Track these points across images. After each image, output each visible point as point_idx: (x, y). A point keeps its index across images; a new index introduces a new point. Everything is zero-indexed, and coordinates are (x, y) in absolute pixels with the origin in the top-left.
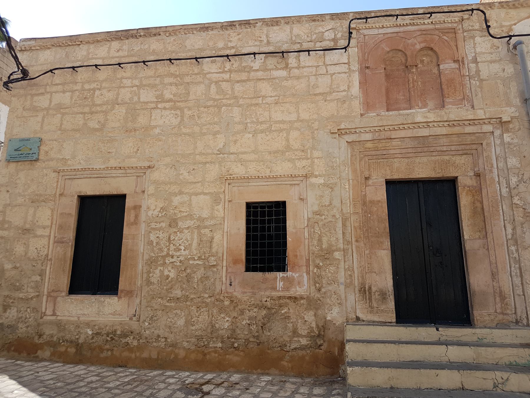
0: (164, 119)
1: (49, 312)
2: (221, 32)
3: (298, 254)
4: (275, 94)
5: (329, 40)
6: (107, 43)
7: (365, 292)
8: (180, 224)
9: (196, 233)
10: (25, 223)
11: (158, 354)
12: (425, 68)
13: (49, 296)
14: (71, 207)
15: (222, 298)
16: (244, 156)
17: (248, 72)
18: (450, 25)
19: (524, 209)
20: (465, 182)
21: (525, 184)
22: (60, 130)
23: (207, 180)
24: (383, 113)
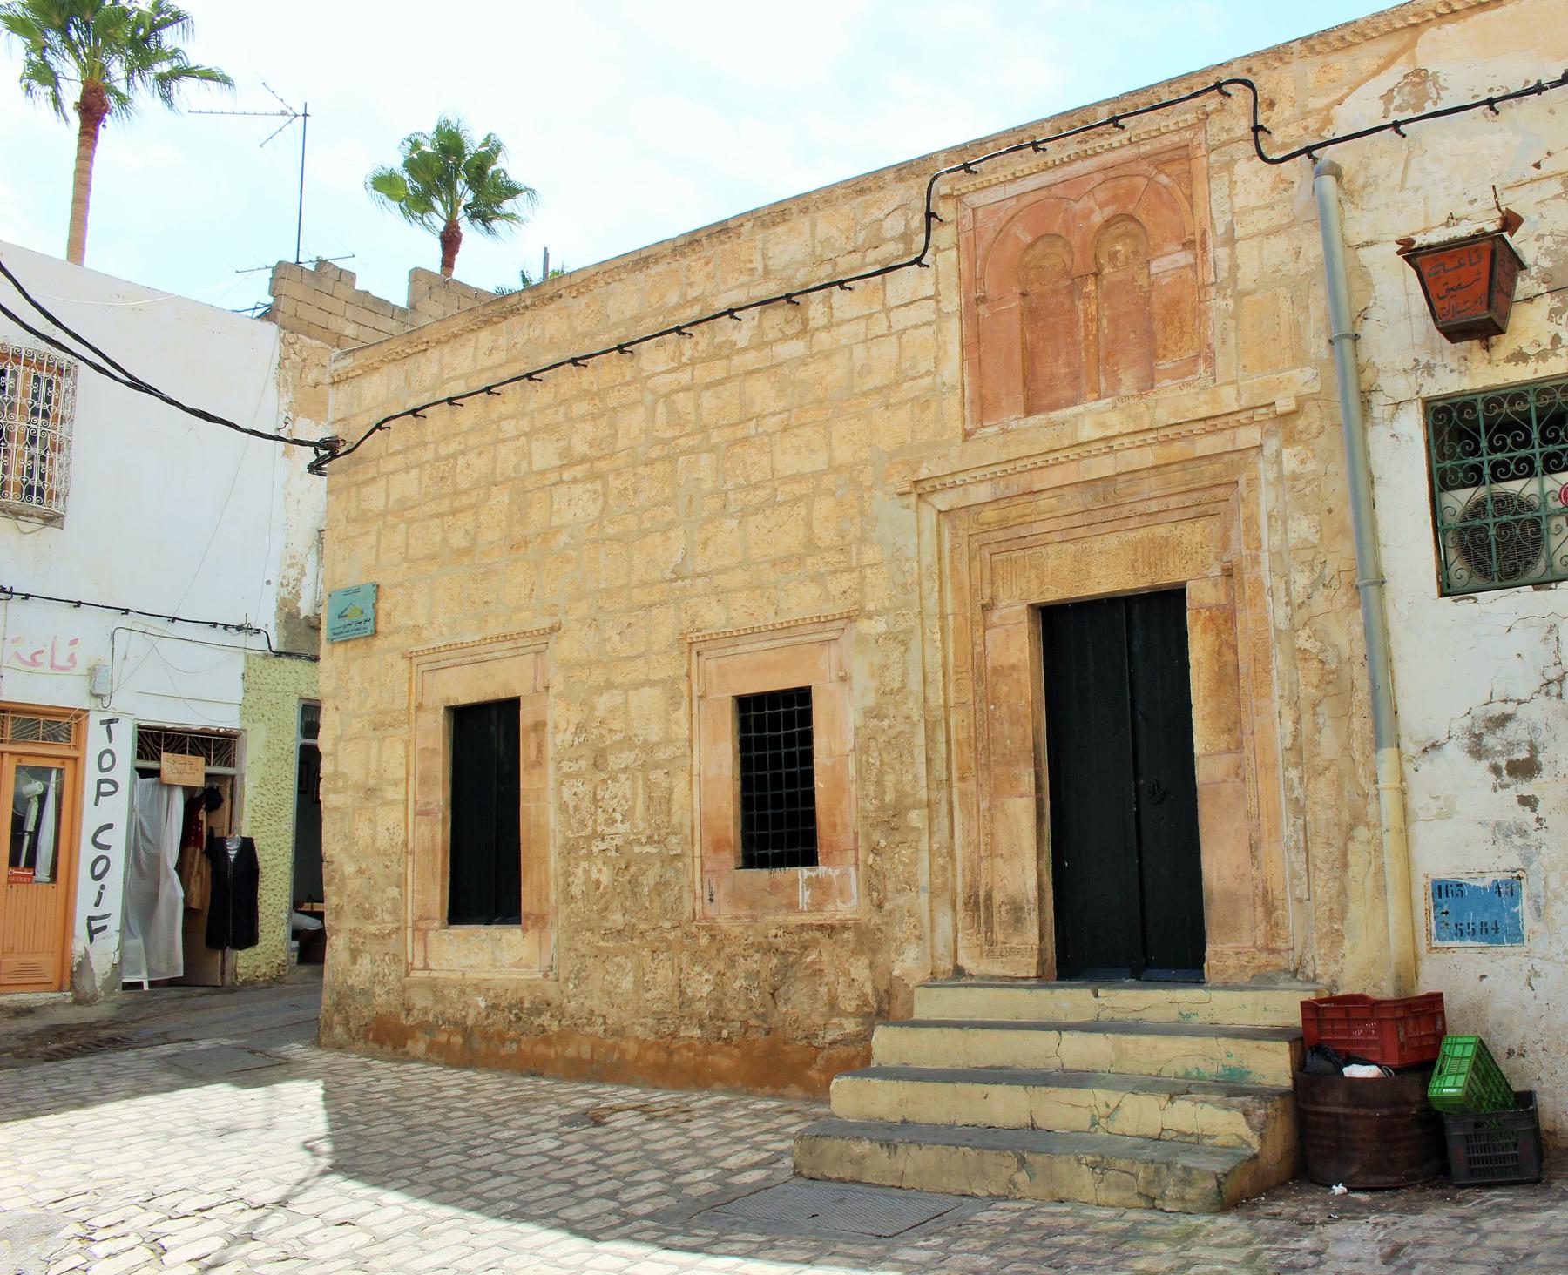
0: (575, 506)
1: (418, 963)
2: (674, 265)
3: (838, 820)
4: (779, 406)
5: (893, 239)
6: (471, 336)
7: (979, 906)
8: (611, 759)
9: (640, 782)
10: (367, 775)
11: (593, 1050)
12: (1120, 276)
13: (415, 929)
14: (434, 734)
15: (694, 930)
16: (721, 580)
17: (728, 357)
18: (1176, 139)
19: (1322, 662)
20: (1201, 595)
21: (1326, 592)
22: (406, 560)
23: (655, 648)
24: (1014, 424)
